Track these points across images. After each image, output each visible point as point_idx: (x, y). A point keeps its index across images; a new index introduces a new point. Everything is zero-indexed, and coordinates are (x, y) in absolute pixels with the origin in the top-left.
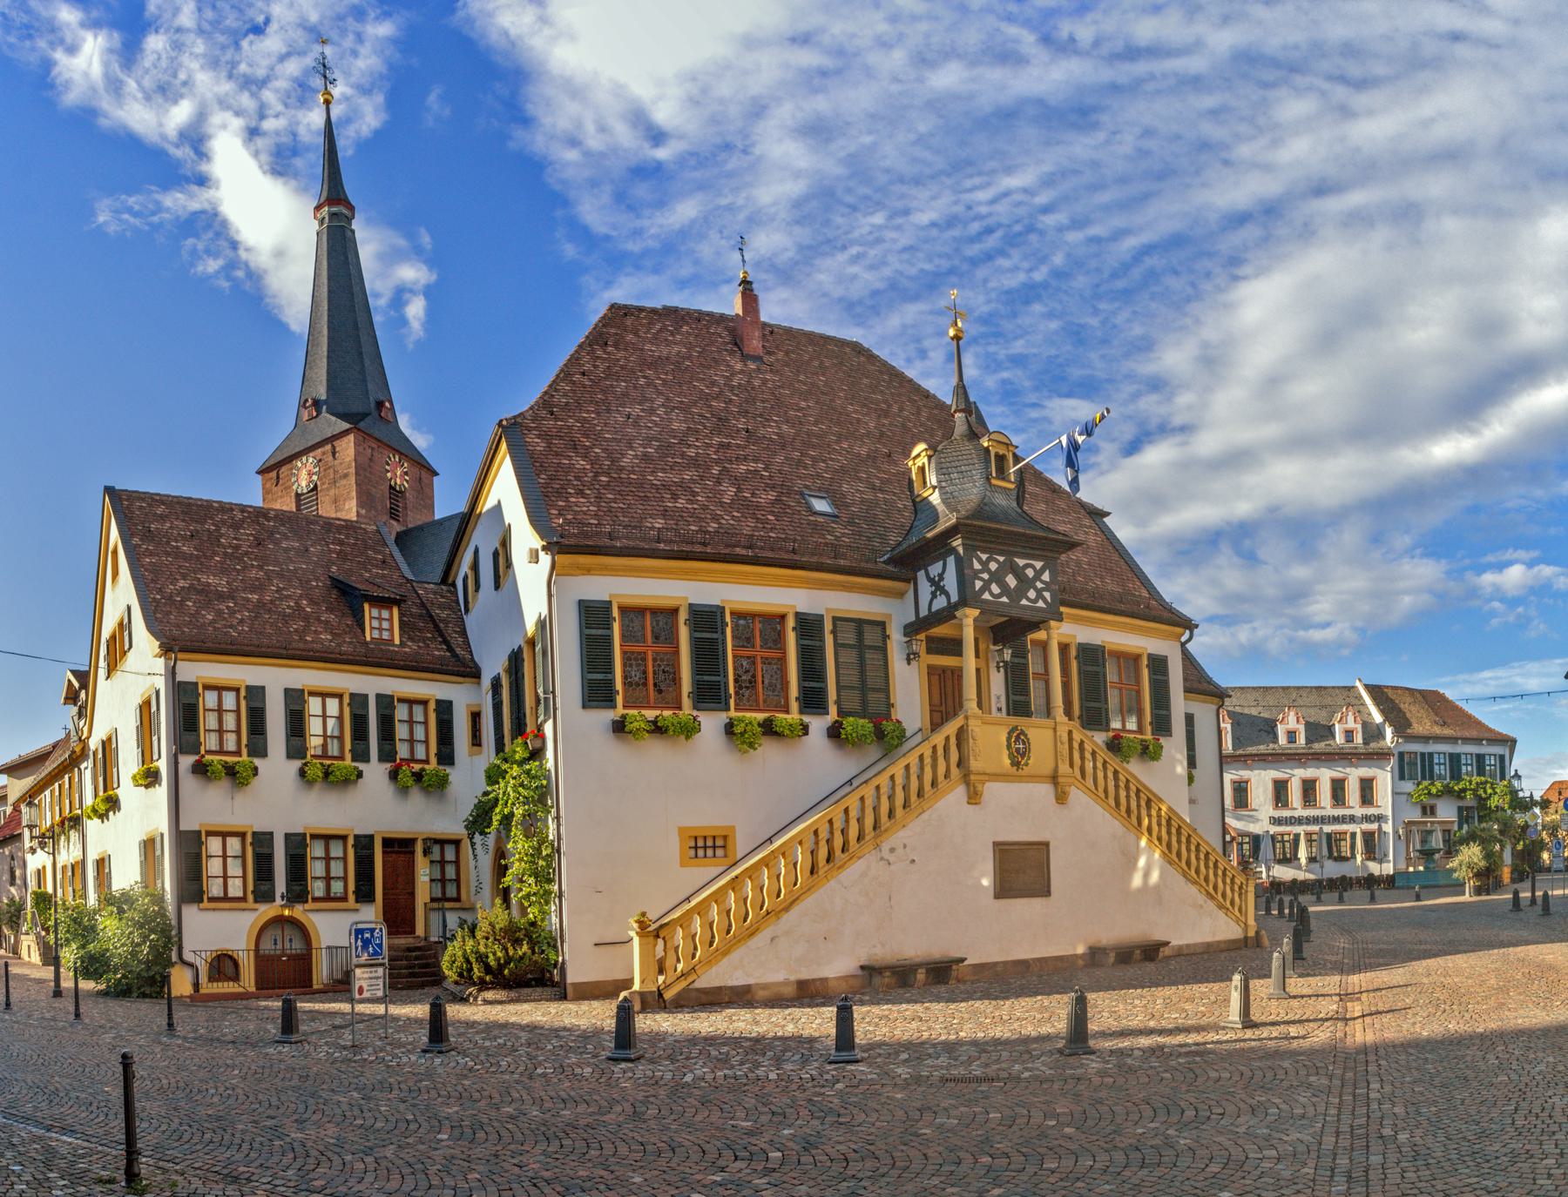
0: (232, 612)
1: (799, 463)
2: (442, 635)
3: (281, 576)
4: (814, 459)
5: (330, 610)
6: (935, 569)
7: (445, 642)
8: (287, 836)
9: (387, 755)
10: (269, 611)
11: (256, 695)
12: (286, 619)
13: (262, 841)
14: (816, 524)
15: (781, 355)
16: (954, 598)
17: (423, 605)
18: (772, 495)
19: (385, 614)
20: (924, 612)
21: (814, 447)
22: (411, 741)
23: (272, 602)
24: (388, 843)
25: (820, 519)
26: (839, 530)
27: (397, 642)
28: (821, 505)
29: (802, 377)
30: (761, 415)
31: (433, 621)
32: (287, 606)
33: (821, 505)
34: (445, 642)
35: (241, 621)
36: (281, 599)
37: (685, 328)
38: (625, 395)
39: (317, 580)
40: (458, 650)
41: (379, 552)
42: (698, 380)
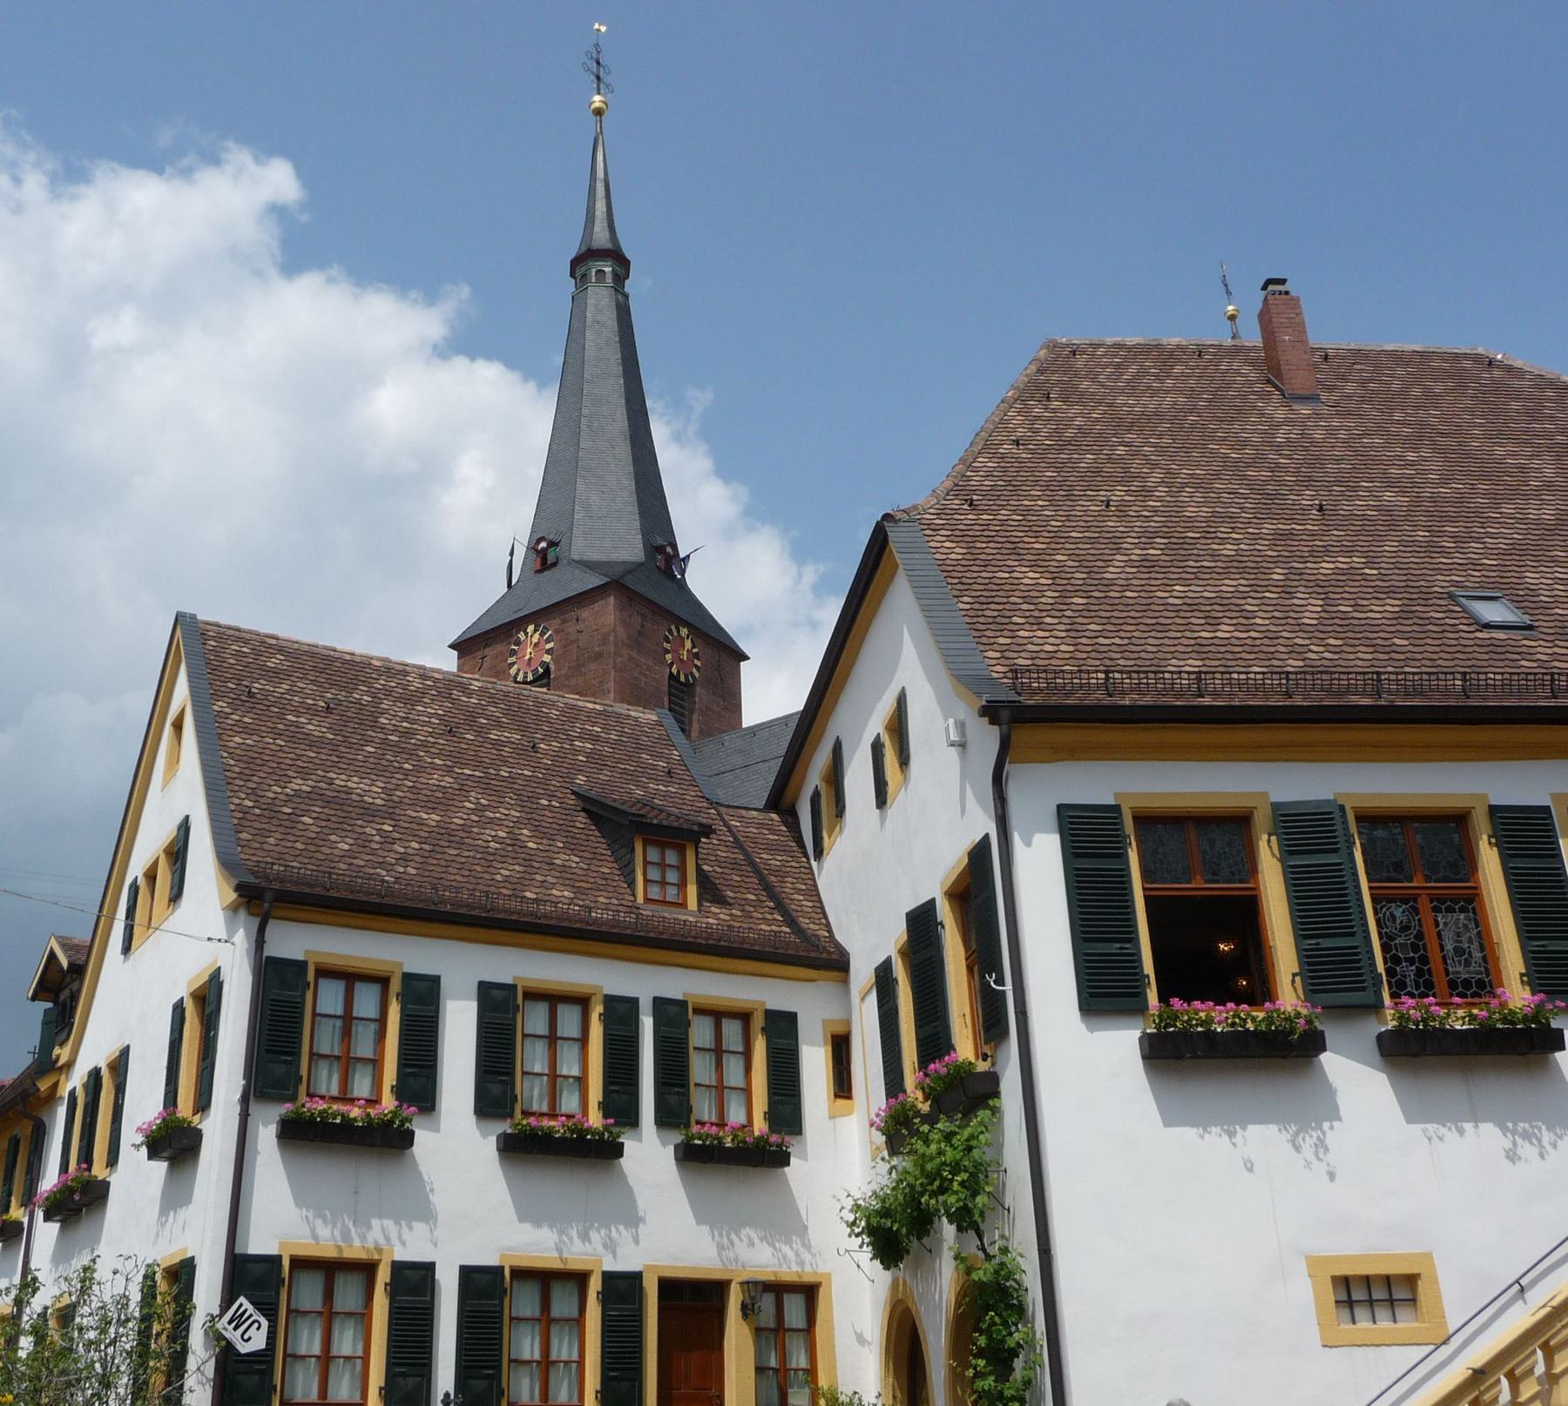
2: (772, 895)
7: (780, 907)
10: (460, 845)
14: (1492, 644)
15: (1350, 388)
17: (738, 844)
18: (1393, 605)
21: (1453, 520)
28: (1493, 612)
29: (1397, 416)
30: (1338, 483)
31: (757, 871)
33: (1493, 612)
34: (780, 907)
35: (404, 859)
37: (1178, 369)
40: (804, 922)
42: (1213, 440)
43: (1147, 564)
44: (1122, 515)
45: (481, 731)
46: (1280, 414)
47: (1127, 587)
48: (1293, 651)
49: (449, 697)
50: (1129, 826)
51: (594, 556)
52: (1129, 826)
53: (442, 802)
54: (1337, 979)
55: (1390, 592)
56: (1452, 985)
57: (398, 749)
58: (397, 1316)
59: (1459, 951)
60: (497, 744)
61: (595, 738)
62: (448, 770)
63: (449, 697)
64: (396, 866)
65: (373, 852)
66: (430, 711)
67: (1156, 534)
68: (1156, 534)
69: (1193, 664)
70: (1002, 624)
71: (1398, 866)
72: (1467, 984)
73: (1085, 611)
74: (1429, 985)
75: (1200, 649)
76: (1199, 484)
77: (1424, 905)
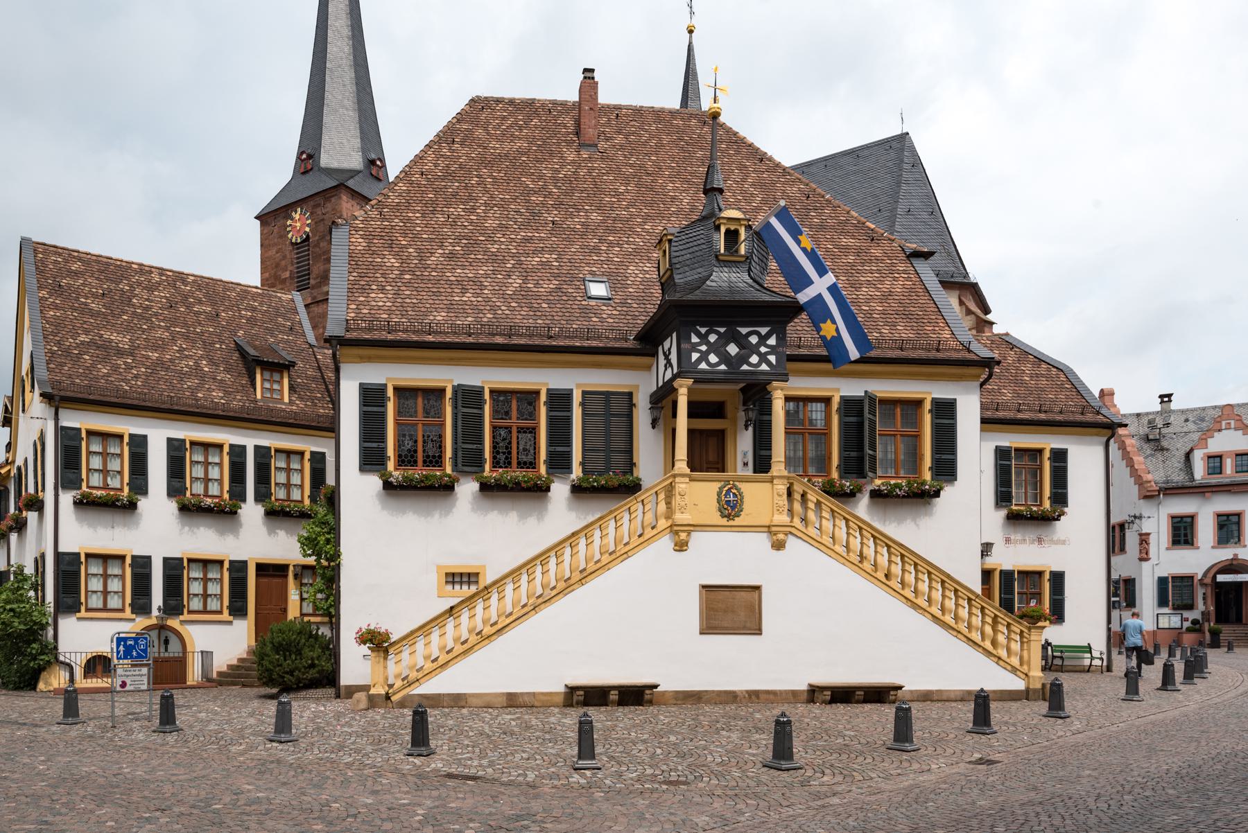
0: (129, 367)
3: (186, 337)
5: (227, 370)
6: (667, 344)
8: (166, 560)
12: (182, 376)
16: (675, 371)
19: (276, 376)
20: (660, 384)
23: (171, 361)
24: (262, 568)
25: (593, 303)
26: (607, 310)
32: (186, 365)
36: (181, 359)
38: (455, 195)
39: (222, 343)
41: (289, 320)
43: (452, 256)
44: (454, 224)
45: (189, 307)
47: (434, 270)
48: (493, 309)
49: (175, 287)
53: (160, 346)
55: (556, 276)
56: (519, 463)
58: (135, 576)
59: (525, 450)
60: (197, 314)
62: (167, 329)
63: (175, 287)
65: (120, 374)
66: (162, 294)
67: (464, 237)
68: (464, 237)
69: (440, 317)
70: (364, 290)
71: (507, 413)
72: (525, 463)
73: (408, 284)
74: (510, 463)
75: (449, 308)
77: (514, 430)
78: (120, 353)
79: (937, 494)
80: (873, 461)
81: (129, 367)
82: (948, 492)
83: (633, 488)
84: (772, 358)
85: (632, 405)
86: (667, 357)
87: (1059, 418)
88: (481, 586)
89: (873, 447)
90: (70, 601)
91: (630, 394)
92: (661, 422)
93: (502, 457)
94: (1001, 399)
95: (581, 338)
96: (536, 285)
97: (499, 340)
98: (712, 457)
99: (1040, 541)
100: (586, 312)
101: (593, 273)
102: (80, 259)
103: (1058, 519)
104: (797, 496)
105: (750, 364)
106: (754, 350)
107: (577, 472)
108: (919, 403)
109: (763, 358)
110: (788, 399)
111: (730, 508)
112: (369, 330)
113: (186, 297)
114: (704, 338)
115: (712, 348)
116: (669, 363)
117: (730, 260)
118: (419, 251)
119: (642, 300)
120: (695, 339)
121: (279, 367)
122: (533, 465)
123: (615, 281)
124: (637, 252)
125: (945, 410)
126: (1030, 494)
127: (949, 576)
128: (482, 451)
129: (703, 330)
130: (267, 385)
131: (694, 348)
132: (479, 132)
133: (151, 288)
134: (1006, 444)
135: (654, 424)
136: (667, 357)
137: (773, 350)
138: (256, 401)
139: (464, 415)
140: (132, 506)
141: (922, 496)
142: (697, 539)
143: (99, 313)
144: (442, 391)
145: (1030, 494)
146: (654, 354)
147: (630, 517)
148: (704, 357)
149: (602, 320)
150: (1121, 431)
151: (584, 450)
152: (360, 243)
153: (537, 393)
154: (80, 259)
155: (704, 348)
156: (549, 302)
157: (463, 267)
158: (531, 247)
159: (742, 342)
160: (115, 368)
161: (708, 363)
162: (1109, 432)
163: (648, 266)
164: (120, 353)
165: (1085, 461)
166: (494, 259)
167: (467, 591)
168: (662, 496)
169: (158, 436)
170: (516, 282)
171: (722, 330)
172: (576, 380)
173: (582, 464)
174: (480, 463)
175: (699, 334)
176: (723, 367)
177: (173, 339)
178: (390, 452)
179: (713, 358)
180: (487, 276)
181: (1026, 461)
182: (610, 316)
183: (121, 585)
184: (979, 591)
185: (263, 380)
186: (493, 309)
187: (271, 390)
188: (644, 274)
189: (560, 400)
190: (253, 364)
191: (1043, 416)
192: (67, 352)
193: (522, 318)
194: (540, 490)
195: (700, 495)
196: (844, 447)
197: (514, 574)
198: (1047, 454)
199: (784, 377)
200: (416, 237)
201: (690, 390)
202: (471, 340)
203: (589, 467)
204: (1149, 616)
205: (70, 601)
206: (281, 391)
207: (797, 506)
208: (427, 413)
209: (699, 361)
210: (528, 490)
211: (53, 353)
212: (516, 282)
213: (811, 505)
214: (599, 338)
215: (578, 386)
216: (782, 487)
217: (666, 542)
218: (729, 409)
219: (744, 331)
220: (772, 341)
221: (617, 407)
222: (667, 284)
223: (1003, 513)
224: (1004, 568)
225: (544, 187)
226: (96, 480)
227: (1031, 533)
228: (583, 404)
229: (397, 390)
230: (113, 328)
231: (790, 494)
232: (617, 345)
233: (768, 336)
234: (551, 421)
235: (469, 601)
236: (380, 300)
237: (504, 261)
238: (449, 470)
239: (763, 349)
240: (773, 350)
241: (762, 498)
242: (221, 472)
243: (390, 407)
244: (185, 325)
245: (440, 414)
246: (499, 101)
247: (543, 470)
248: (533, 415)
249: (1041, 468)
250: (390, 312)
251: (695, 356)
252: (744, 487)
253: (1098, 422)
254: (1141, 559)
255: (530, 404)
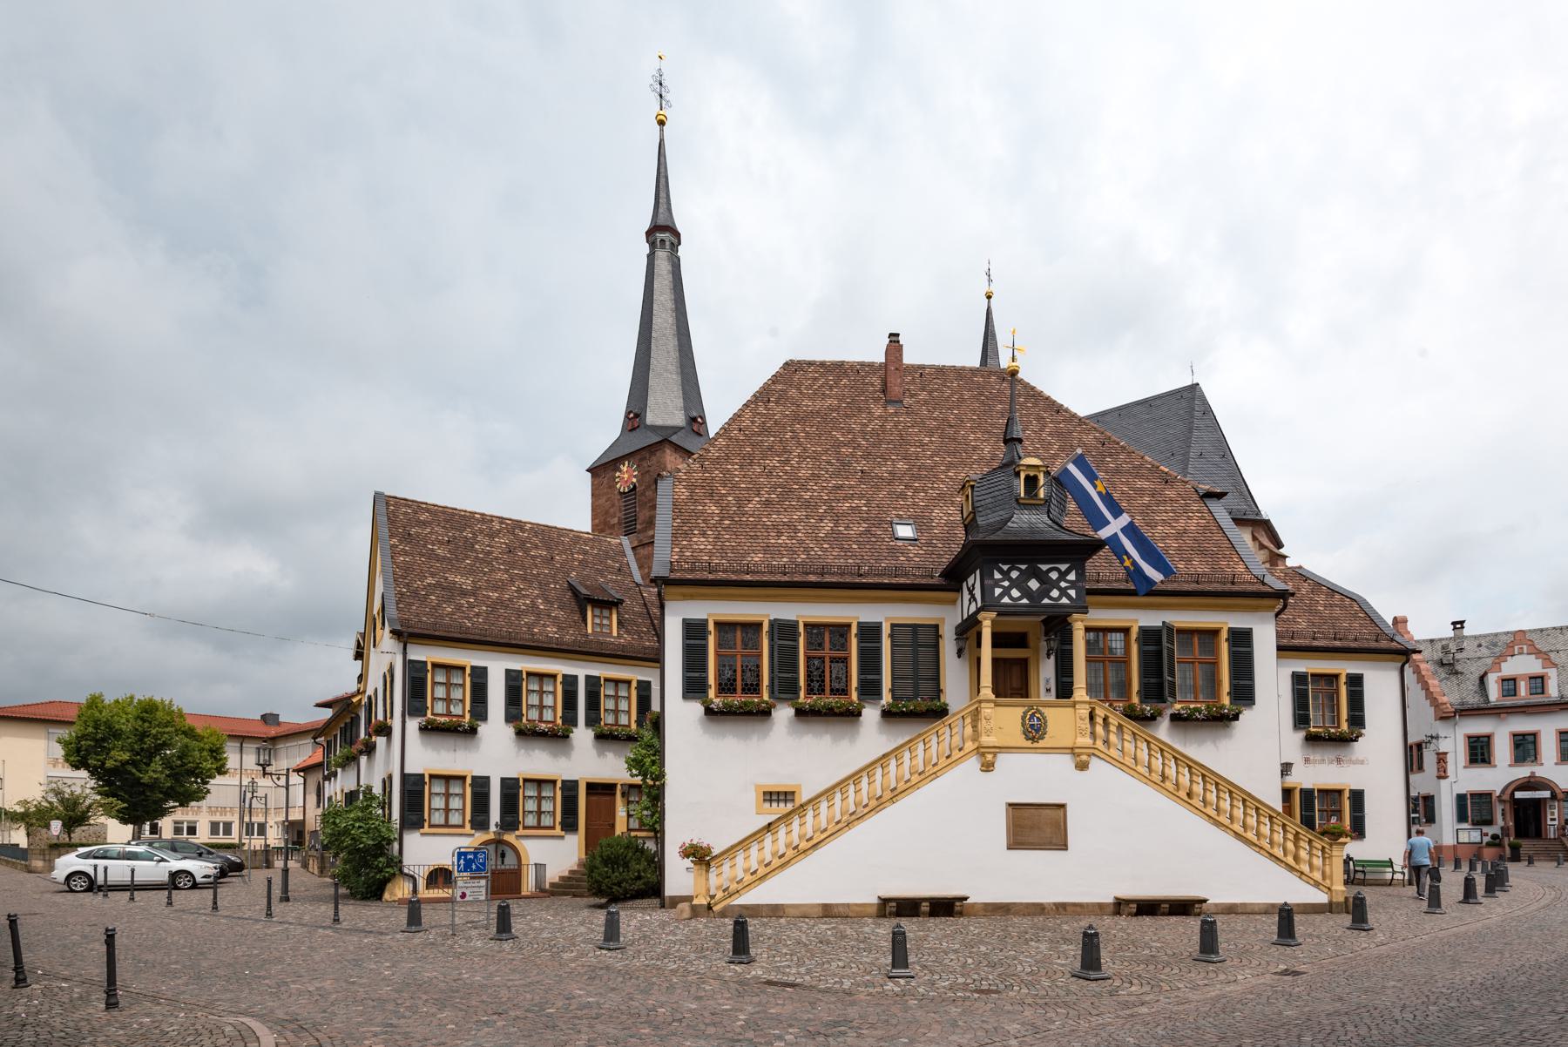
0: (471, 606)
1: (902, 496)
4: (916, 490)
6: (971, 580)
8: (503, 780)
9: (592, 721)
11: (570, 681)
13: (481, 784)
19: (606, 613)
21: (918, 478)
22: (616, 712)
25: (900, 543)
26: (913, 550)
27: (615, 634)
35: (478, 615)
36: (518, 598)
43: (768, 503)
45: (526, 551)
46: (878, 412)
48: (807, 550)
50: (711, 627)
51: (659, 422)
52: (711, 627)
53: (500, 587)
54: (785, 689)
57: (482, 561)
60: (533, 557)
61: (585, 553)
62: (506, 571)
64: (474, 619)
71: (820, 645)
76: (815, 457)
77: (827, 660)
78: (464, 593)
79: (1236, 717)
80: (1174, 687)
81: (471, 606)
82: (1247, 715)
83: (941, 713)
84: (1072, 593)
85: (938, 637)
86: (971, 592)
87: (1353, 645)
88: (797, 804)
89: (1172, 674)
90: (414, 818)
91: (937, 626)
92: (966, 651)
93: (816, 685)
94: (1296, 628)
95: (890, 576)
96: (847, 528)
97: (812, 578)
98: (1016, 683)
99: (1339, 761)
100: (893, 551)
101: (900, 517)
102: (428, 511)
103: (1356, 740)
104: (1099, 720)
105: (1051, 598)
106: (1055, 584)
107: (887, 698)
108: (1215, 633)
109: (1063, 592)
110: (1088, 630)
111: (1034, 731)
112: (692, 570)
113: (524, 543)
114: (1006, 575)
115: (1015, 584)
116: (973, 598)
117: (1030, 501)
118: (738, 499)
119: (946, 540)
120: (997, 576)
121: (608, 605)
122: (845, 691)
123: (920, 522)
124: (941, 497)
125: (1242, 639)
126: (1328, 717)
127: (1249, 795)
128: (796, 680)
129: (1005, 568)
130: (597, 621)
131: (997, 583)
132: (793, 392)
133: (492, 535)
134: (1302, 669)
135: (960, 653)
136: (971, 592)
137: (1073, 585)
138: (587, 635)
139: (780, 646)
140: (472, 731)
141: (1222, 720)
142: (1003, 760)
143: (444, 558)
144: (759, 625)
145: (1328, 717)
146: (959, 590)
147: (938, 740)
148: (1006, 592)
149: (909, 559)
150: (1415, 656)
151: (893, 678)
152: (683, 493)
153: (849, 626)
154: (428, 511)
155: (1006, 584)
156: (859, 543)
157: (778, 513)
158: (841, 494)
159: (1042, 578)
160: (459, 607)
161: (1011, 598)
162: (1404, 658)
163: (952, 510)
164: (464, 593)
165: (1381, 685)
166: (807, 505)
167: (784, 808)
168: (968, 720)
169: (497, 667)
170: (828, 525)
171: (1023, 567)
172: (885, 614)
173: (892, 691)
174: (794, 690)
175: (1001, 571)
176: (1025, 601)
177: (512, 581)
178: (711, 680)
179: (1015, 593)
180: (800, 521)
181: (1323, 686)
182: (916, 555)
183: (462, 803)
184: (1280, 810)
185: (594, 616)
186: (807, 550)
187: (601, 625)
188: (948, 516)
189: (870, 633)
190: (584, 601)
191: (1338, 644)
192: (415, 593)
193: (834, 558)
194: (853, 714)
195: (1005, 720)
196: (1144, 674)
197: (828, 793)
198: (1343, 679)
199: (1084, 610)
200: (735, 486)
201: (994, 622)
202: (786, 578)
203: (898, 693)
204: (1448, 829)
205: (414, 818)
206: (610, 626)
207: (1099, 729)
208: (745, 645)
209: (1002, 596)
210: (841, 714)
211: (402, 594)
212: (828, 525)
213: (1113, 728)
214: (906, 575)
215: (887, 619)
216: (1084, 711)
217: (973, 763)
218: (1031, 639)
219: (1044, 567)
220: (1072, 577)
221: (923, 638)
222: (970, 525)
223: (1301, 734)
224: (1305, 786)
225: (854, 440)
226: (440, 708)
227: (1329, 753)
228: (891, 636)
229: (717, 624)
230: (458, 571)
231: (1092, 717)
232: (924, 581)
233: (1068, 571)
234: (861, 651)
235: (786, 818)
236: (701, 543)
237: (816, 507)
238: (766, 697)
239: (1063, 584)
240: (1073, 585)
241: (1064, 722)
242: (554, 698)
243: (711, 640)
244: (523, 567)
245: (758, 646)
246: (810, 363)
247: (854, 696)
248: (845, 646)
249: (1337, 692)
250: (711, 554)
251: (998, 591)
252: (1047, 711)
253: (1393, 649)
254: (1439, 777)
255: (841, 636)
